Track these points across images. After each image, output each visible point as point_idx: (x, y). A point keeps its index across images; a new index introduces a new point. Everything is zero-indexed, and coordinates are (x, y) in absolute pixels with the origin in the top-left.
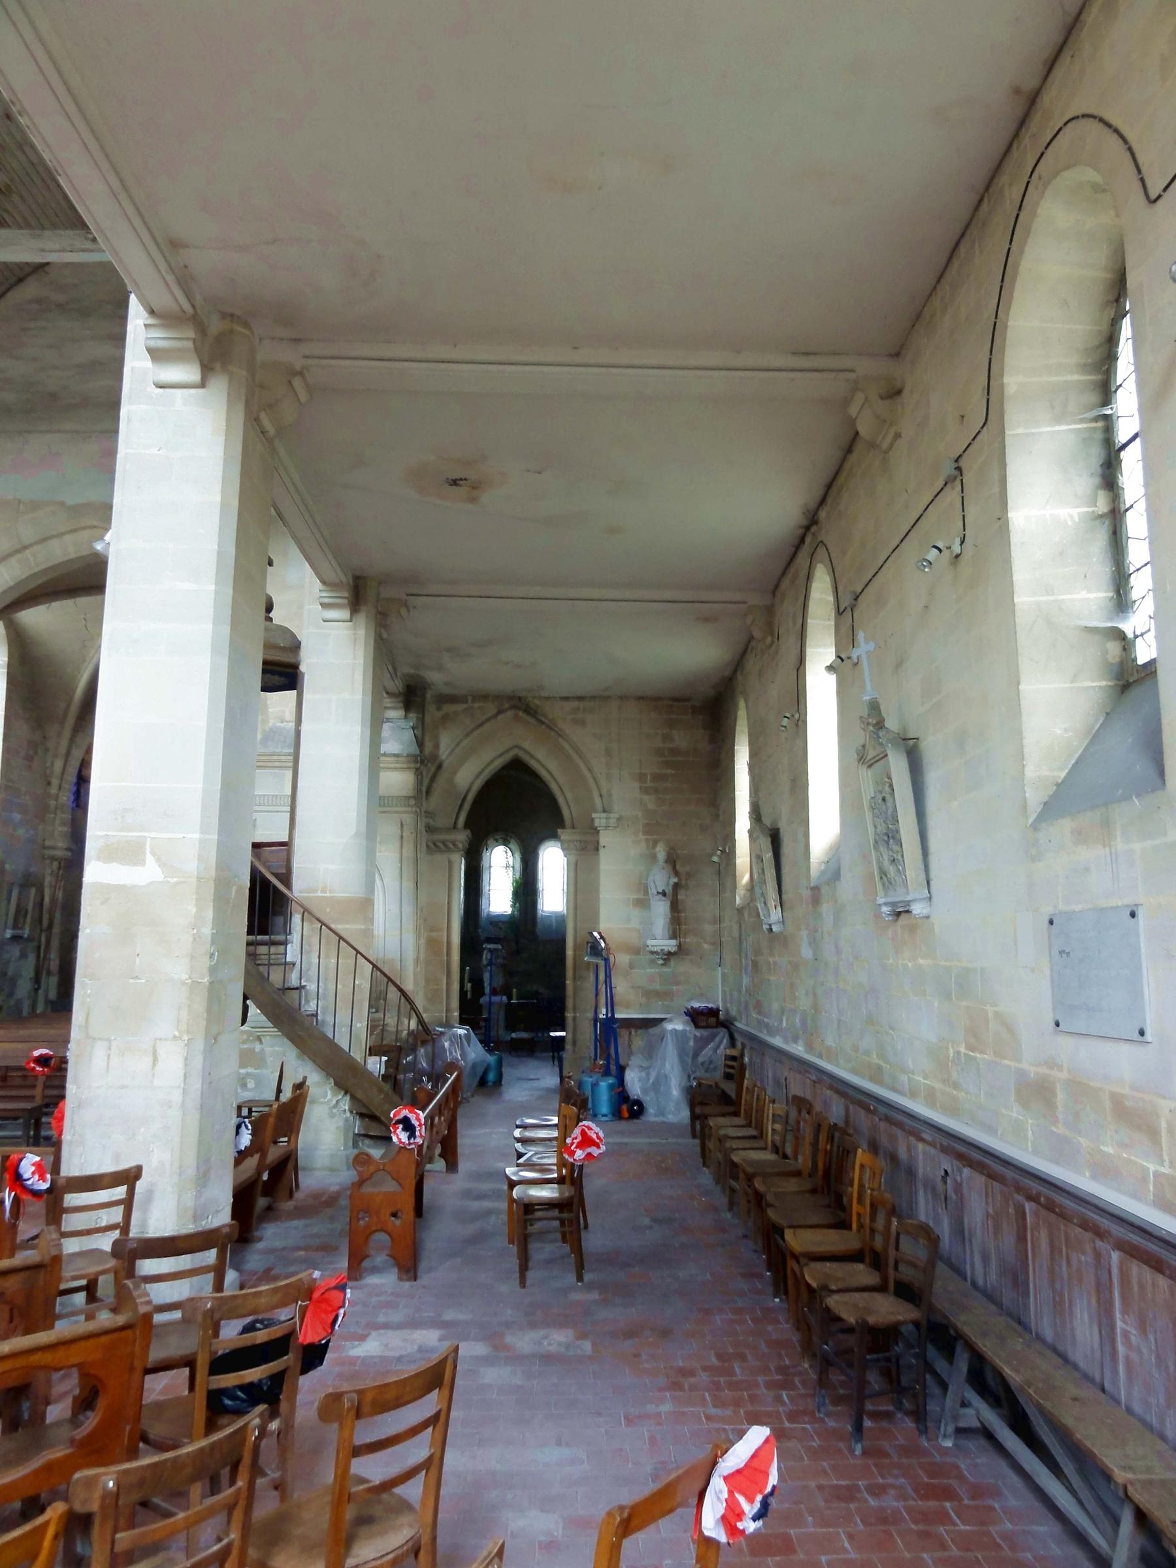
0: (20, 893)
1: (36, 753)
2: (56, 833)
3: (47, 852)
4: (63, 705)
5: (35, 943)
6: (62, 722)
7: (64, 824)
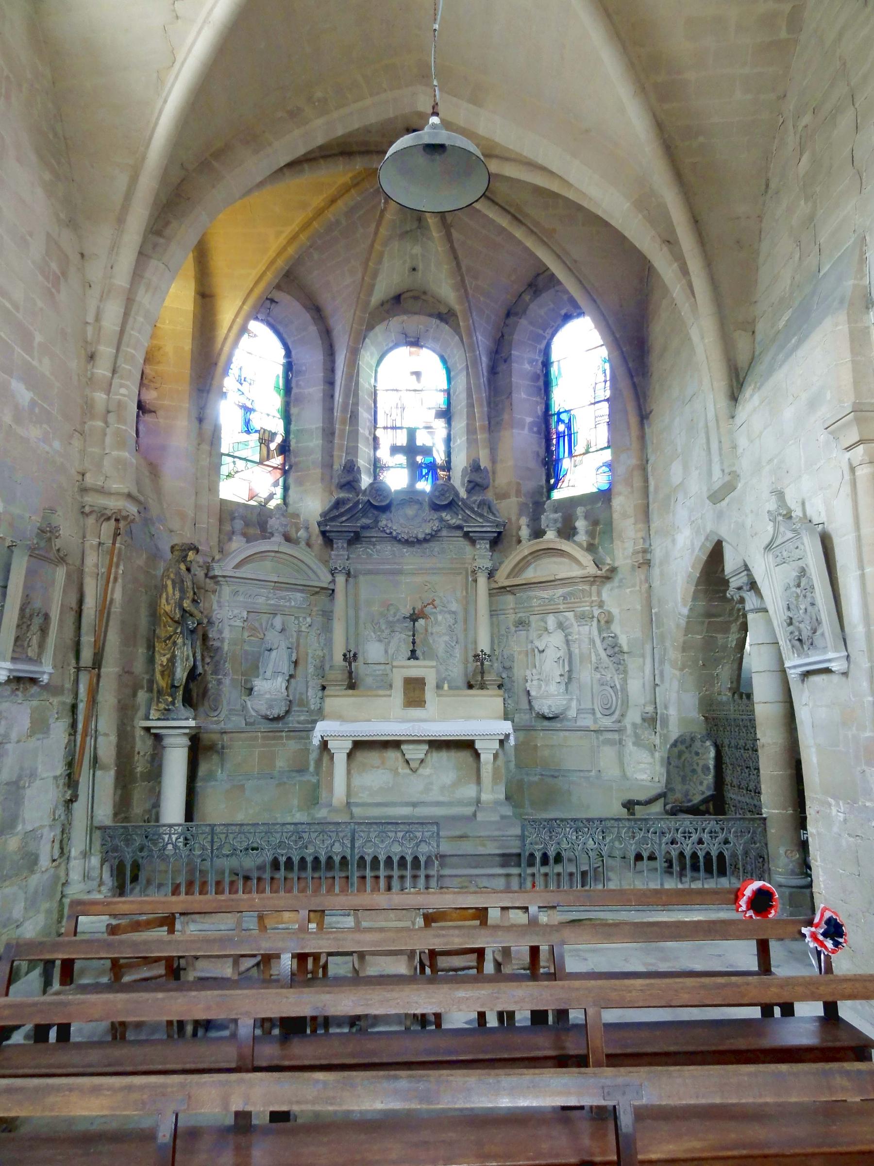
0: (30, 573)
1: (64, 274)
2: (106, 462)
3: (89, 499)
4: (122, 181)
5: (69, 700)
6: (121, 220)
7: (121, 444)
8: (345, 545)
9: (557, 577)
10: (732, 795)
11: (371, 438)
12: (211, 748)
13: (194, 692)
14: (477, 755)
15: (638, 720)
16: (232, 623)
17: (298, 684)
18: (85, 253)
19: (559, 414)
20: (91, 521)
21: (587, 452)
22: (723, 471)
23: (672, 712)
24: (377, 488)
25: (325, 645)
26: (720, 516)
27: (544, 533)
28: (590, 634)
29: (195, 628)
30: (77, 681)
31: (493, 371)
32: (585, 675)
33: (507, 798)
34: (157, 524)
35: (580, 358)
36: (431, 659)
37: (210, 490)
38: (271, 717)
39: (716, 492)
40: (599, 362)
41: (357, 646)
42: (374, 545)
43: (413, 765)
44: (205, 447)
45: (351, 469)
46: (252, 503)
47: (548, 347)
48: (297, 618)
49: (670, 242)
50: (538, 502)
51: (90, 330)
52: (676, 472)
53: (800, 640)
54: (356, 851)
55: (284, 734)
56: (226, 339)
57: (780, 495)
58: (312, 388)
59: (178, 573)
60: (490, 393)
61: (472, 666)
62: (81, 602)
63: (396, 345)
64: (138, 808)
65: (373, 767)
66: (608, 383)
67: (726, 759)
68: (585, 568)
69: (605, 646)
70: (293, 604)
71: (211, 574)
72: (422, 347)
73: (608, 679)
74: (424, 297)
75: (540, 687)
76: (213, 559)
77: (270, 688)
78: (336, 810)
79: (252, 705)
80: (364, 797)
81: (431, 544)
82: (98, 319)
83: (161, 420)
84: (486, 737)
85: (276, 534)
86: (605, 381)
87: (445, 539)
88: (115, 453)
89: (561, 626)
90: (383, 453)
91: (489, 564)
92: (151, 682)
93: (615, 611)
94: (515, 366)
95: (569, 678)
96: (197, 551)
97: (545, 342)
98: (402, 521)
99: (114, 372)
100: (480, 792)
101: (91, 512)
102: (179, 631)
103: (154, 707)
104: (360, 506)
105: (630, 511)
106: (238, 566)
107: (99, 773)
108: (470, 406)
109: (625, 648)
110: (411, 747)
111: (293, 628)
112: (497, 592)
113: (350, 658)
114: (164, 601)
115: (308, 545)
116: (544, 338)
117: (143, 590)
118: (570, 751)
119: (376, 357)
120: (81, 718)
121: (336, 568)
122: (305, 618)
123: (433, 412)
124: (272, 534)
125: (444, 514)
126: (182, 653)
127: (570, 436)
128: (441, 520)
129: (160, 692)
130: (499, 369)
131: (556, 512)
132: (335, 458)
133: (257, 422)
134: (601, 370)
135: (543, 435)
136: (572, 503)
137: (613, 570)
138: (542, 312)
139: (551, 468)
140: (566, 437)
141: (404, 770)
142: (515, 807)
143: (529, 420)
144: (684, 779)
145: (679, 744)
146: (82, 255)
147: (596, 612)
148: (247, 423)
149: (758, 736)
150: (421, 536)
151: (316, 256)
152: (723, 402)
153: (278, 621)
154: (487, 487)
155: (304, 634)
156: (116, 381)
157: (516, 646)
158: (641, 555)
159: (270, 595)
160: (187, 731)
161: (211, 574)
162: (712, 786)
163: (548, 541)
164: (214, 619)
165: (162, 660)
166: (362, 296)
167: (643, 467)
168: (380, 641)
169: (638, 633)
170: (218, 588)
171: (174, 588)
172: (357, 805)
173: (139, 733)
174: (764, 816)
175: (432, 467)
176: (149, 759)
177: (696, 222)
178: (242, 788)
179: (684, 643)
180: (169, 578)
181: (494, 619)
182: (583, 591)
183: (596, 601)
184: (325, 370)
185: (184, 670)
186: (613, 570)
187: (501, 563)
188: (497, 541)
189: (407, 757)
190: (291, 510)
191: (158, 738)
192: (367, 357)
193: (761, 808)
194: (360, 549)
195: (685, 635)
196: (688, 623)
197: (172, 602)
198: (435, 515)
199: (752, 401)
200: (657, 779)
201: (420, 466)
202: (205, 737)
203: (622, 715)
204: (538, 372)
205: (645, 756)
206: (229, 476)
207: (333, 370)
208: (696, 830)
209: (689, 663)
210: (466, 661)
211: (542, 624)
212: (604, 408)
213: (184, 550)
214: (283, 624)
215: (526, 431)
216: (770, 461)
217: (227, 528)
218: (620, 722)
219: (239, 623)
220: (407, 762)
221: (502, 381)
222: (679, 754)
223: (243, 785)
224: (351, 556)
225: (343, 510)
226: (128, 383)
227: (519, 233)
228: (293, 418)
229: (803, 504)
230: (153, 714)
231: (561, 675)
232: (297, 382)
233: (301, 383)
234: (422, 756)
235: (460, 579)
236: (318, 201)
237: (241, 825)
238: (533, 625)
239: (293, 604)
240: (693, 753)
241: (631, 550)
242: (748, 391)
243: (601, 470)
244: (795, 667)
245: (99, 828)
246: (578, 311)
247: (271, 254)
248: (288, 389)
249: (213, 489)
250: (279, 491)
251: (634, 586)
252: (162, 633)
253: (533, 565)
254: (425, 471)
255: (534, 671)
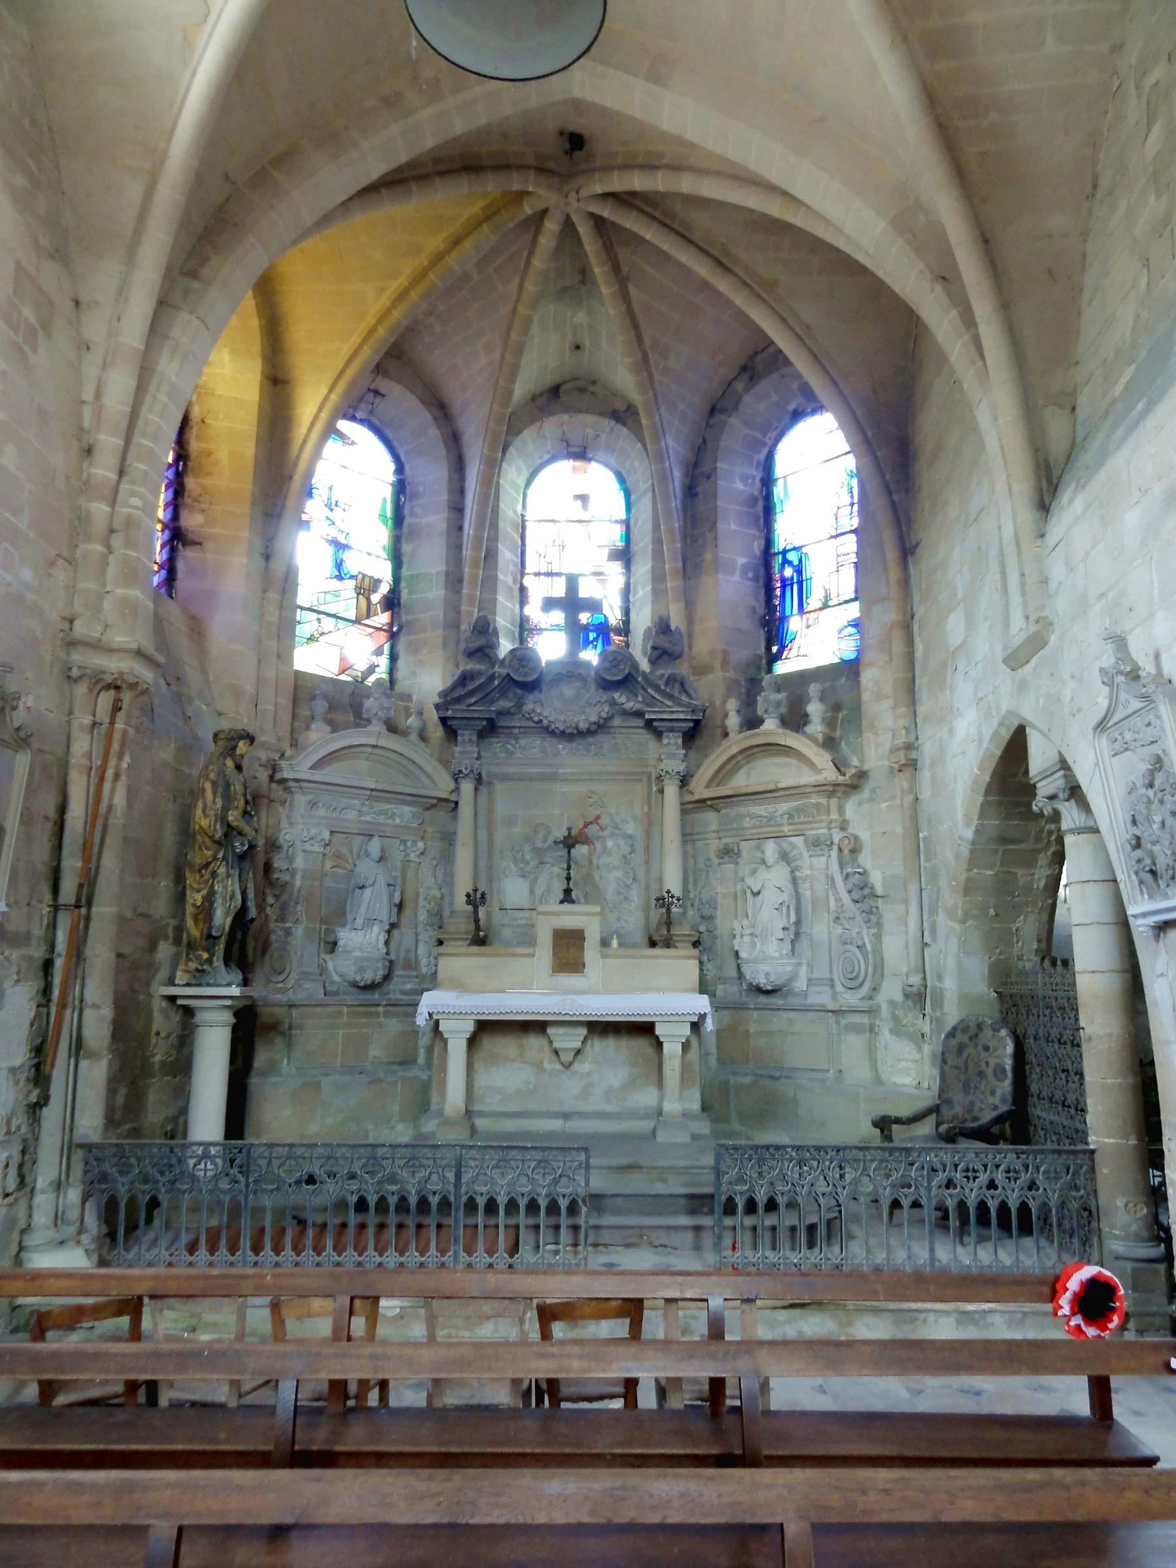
1: (46, 326)
2: (107, 604)
3: (78, 657)
4: (134, 192)
5: (38, 953)
6: (131, 251)
8: (474, 738)
9: (780, 785)
10: (1040, 1112)
11: (516, 588)
12: (274, 1028)
13: (245, 946)
14: (659, 1045)
15: (899, 997)
16: (307, 847)
17: (405, 936)
18: (81, 299)
19: (785, 552)
20: (81, 690)
21: (825, 606)
22: (1027, 618)
23: (949, 985)
24: (522, 657)
25: (444, 881)
26: (1022, 687)
27: (761, 722)
28: (827, 868)
29: (245, 852)
30: (53, 925)
31: (690, 491)
32: (820, 929)
33: (705, 1108)
34: (197, 702)
35: (816, 472)
36: (595, 903)
37: (279, 656)
38: (362, 984)
39: (1015, 651)
40: (844, 477)
41: (490, 881)
42: (517, 739)
43: (567, 1057)
44: (273, 595)
45: (484, 629)
46: (344, 677)
47: (770, 457)
48: (404, 842)
49: (947, 277)
50: (754, 675)
51: (87, 412)
52: (955, 627)
53: (1153, 872)
54: (464, 1189)
55: (381, 1009)
56: (305, 442)
57: (1120, 643)
58: (432, 517)
59: (221, 772)
60: (685, 523)
61: (657, 914)
62: (62, 809)
63: (554, 458)
64: (155, 1112)
65: (507, 1059)
66: (856, 507)
67: (1030, 1057)
68: (820, 771)
69: (850, 886)
70: (398, 821)
71: (278, 776)
72: (590, 460)
73: (854, 935)
74: (592, 388)
75: (754, 945)
76: (283, 755)
77: (362, 942)
78: (447, 1122)
79: (334, 968)
80: (492, 1103)
81: (599, 738)
82: (98, 395)
83: (209, 556)
84: (672, 1018)
85: (375, 722)
86: (852, 505)
87: (618, 730)
88: (120, 591)
89: (784, 857)
90: (533, 610)
91: (681, 767)
92: (180, 929)
93: (864, 835)
94: (722, 484)
95: (796, 933)
96: (251, 739)
97: (766, 451)
98: (557, 704)
99: (121, 473)
100: (661, 1099)
101: (81, 677)
102: (220, 855)
103: (182, 967)
104: (496, 682)
105: (887, 689)
106: (315, 766)
107: (83, 1063)
108: (657, 542)
109: (879, 890)
110: (561, 1031)
111: (397, 856)
112: (691, 808)
113: (476, 900)
114: (199, 812)
115: (423, 737)
116: (765, 444)
117: (171, 796)
118: (798, 1042)
119: (525, 474)
120: (57, 980)
121: (460, 771)
122: (415, 842)
123: (605, 553)
124: (369, 721)
125: (616, 695)
126: (225, 888)
127: (800, 583)
128: (613, 703)
129: (191, 946)
130: (700, 489)
131: (779, 691)
132: (464, 616)
133: (354, 563)
134: (846, 488)
135: (761, 582)
136: (803, 678)
137: (862, 775)
138: (762, 407)
139: (773, 631)
140: (795, 587)
141: (550, 1064)
142: (715, 1120)
143: (741, 561)
144: (966, 1087)
145: (958, 1033)
146: (77, 303)
147: (837, 836)
148: (339, 565)
149: (1082, 1023)
150: (583, 726)
151: (437, 328)
152: (1027, 515)
153: (375, 846)
154: (679, 656)
155: (412, 865)
156: (124, 486)
157: (720, 884)
158: (902, 753)
159: (365, 809)
160: (228, 1002)
161: (278, 776)
162: (1010, 1098)
163: (767, 733)
164: (281, 840)
165: (196, 898)
166: (501, 383)
167: (907, 626)
168: (524, 876)
169: (898, 867)
170: (289, 796)
171: (214, 793)
172: (482, 1114)
173: (158, 1005)
174: (1092, 1147)
175: (603, 630)
176: (175, 1042)
177: (986, 242)
178: (317, 1086)
179: (968, 880)
180: (207, 778)
181: (689, 847)
182: (817, 805)
183: (836, 820)
184: (451, 491)
185: (227, 914)
186: (862, 775)
187: (698, 766)
188: (694, 733)
189: (557, 1045)
190: (399, 688)
191: (188, 1012)
192: (512, 474)
193: (1085, 1134)
194: (496, 745)
195: (969, 870)
196: (972, 852)
197: (212, 813)
198: (605, 696)
199: (1073, 506)
200: (926, 1085)
201: (586, 628)
202: (265, 1013)
203: (874, 989)
204: (756, 493)
205: (908, 1049)
206: (311, 639)
207: (462, 492)
208: (985, 1166)
209: (975, 912)
210: (647, 908)
211: (759, 854)
212: (850, 544)
213: (232, 739)
214: (383, 850)
215: (737, 577)
216: (1102, 595)
217: (304, 712)
218: (870, 998)
219: (317, 848)
220: (556, 1053)
221: (704, 502)
222: (959, 1051)
223: (319, 1083)
224: (483, 754)
225: (471, 688)
226: (142, 490)
227: (723, 285)
228: (405, 559)
229: (1157, 657)
230: (181, 977)
231: (784, 929)
232: (412, 508)
233: (418, 510)
234: (578, 1044)
235: (639, 789)
236: (435, 242)
237: (291, 1146)
238: (745, 854)
239: (398, 821)
240: (980, 1047)
241: (887, 746)
242: (1065, 496)
243: (845, 632)
244: (1145, 915)
245: (80, 1146)
246: (814, 405)
247: (370, 319)
248: (398, 519)
249: (284, 655)
250: (383, 662)
251: (893, 798)
252: (197, 857)
253: (745, 769)
254: (592, 636)
255: (745, 922)
